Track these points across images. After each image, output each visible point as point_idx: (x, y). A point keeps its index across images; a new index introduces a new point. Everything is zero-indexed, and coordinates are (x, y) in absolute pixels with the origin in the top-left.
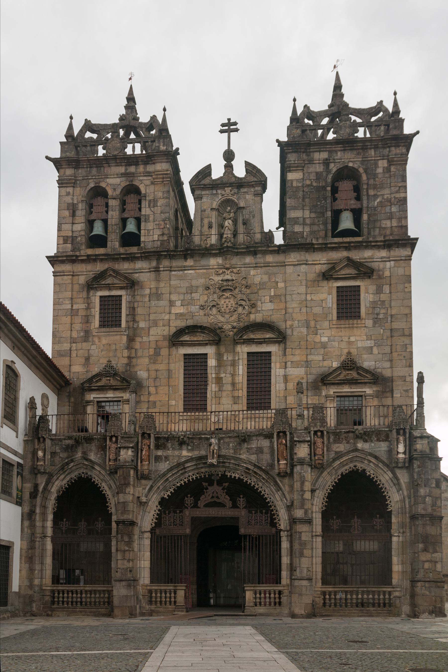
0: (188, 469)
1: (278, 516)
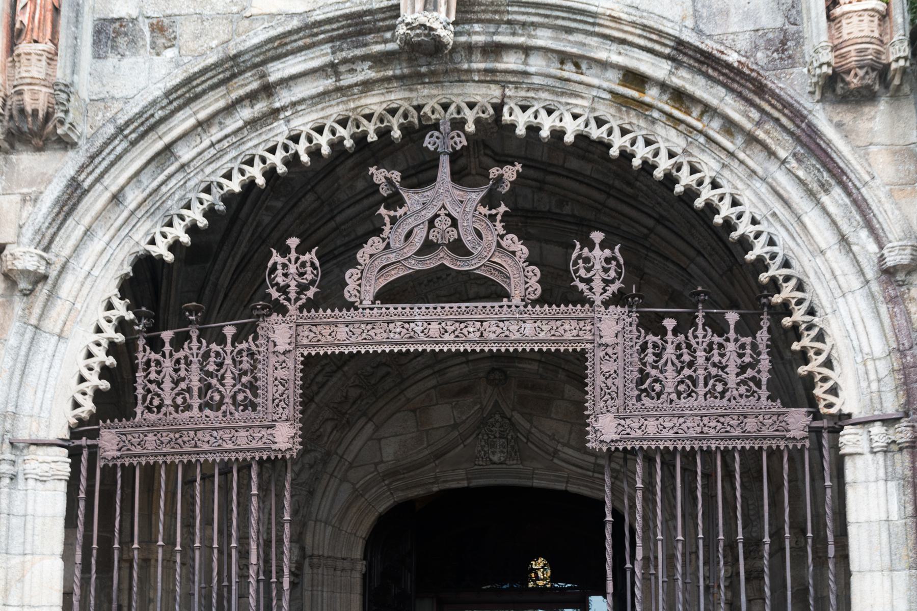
0: (284, 97)
1: (820, 337)
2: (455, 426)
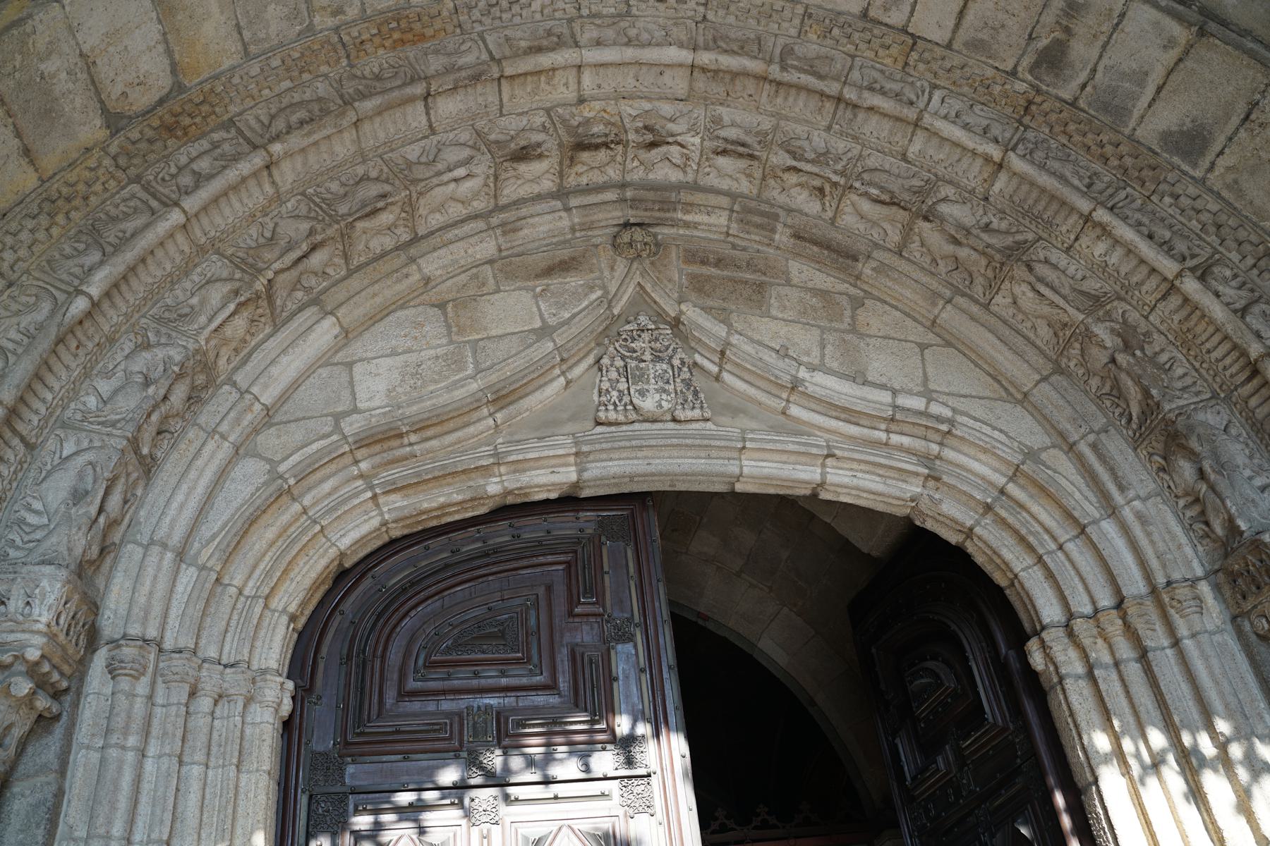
2: (545, 331)
